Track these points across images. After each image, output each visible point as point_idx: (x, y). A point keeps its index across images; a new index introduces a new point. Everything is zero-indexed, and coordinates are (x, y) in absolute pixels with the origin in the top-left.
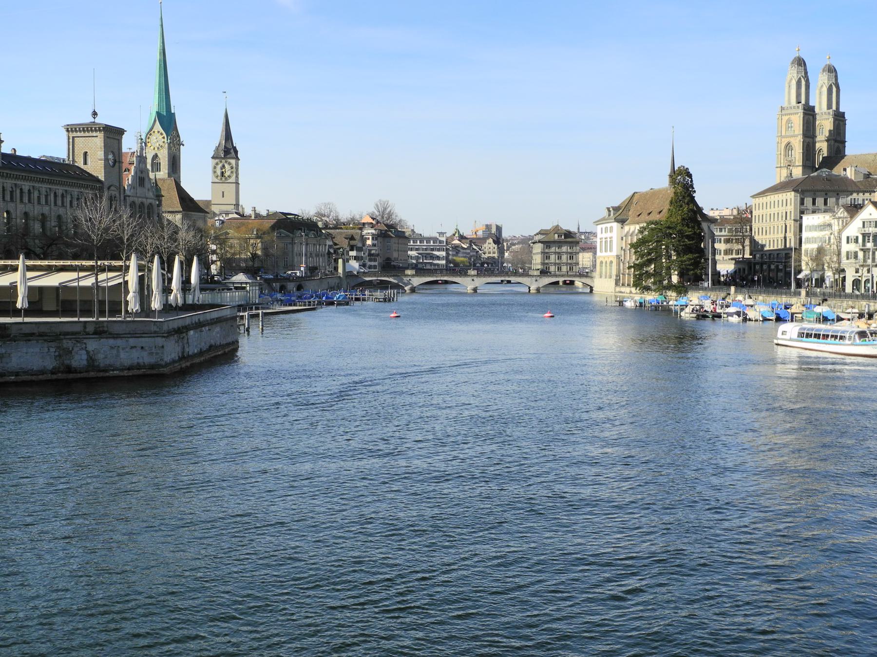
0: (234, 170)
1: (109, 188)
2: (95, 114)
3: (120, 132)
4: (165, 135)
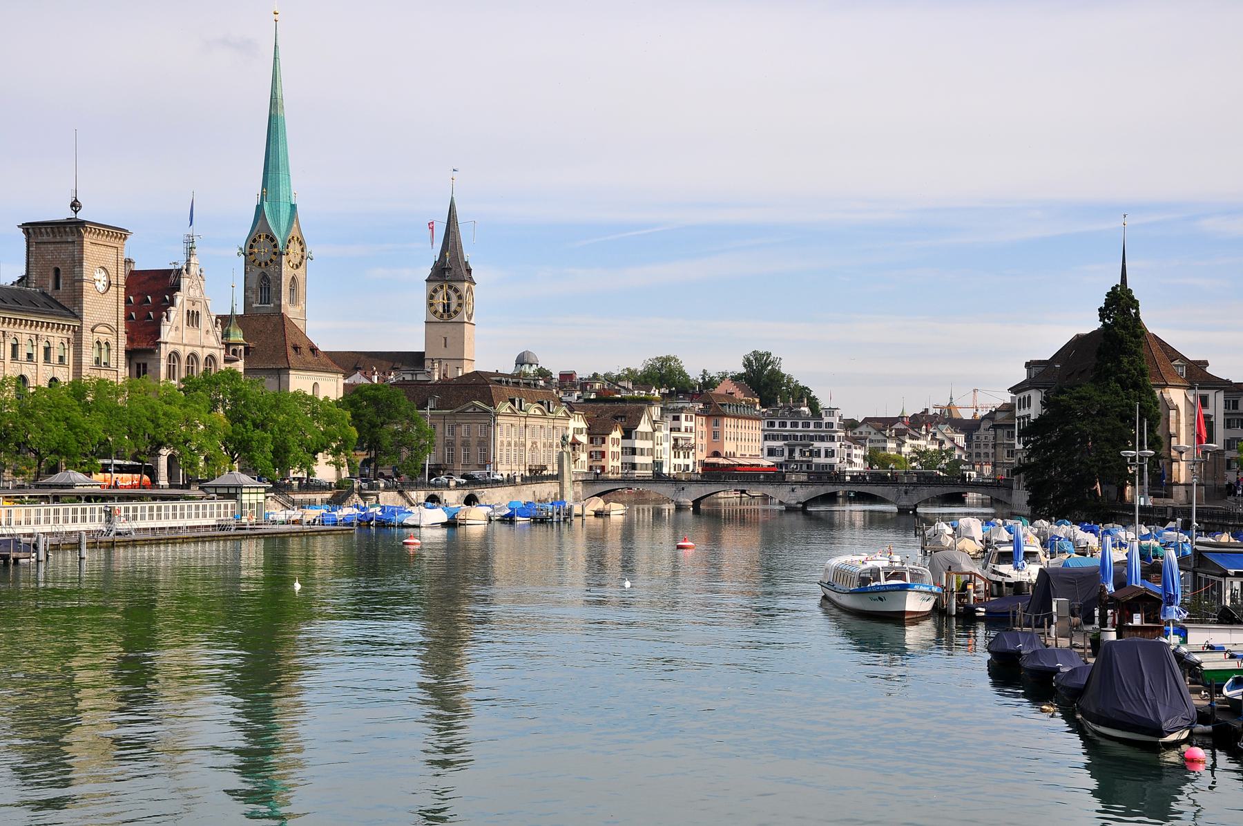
2: (75, 205)
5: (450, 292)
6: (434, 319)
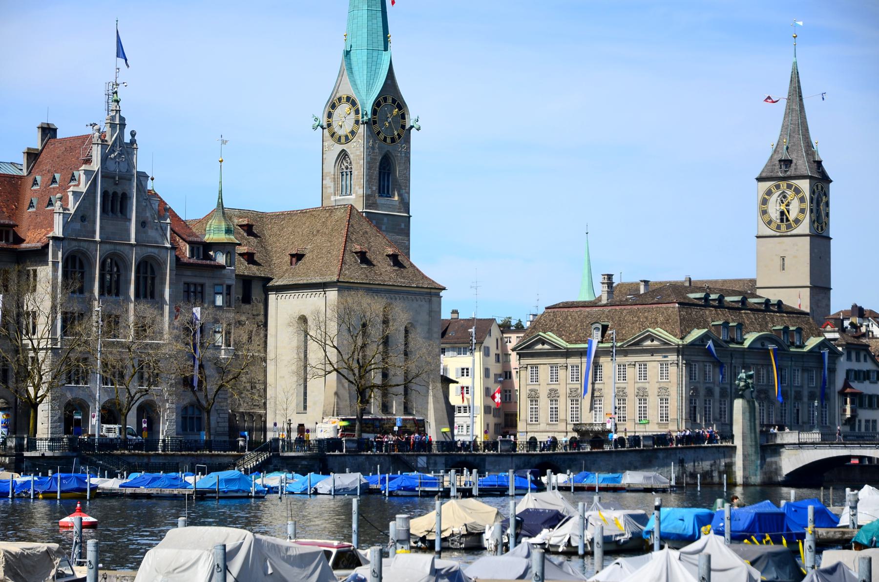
0: (807, 205)
5: (790, 193)
6: (769, 232)
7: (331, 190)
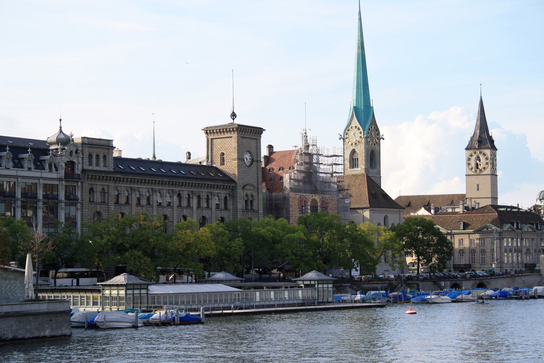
1: (243, 188)
2: (234, 115)
3: (259, 131)
4: (361, 130)
6: (471, 173)
7: (348, 166)
